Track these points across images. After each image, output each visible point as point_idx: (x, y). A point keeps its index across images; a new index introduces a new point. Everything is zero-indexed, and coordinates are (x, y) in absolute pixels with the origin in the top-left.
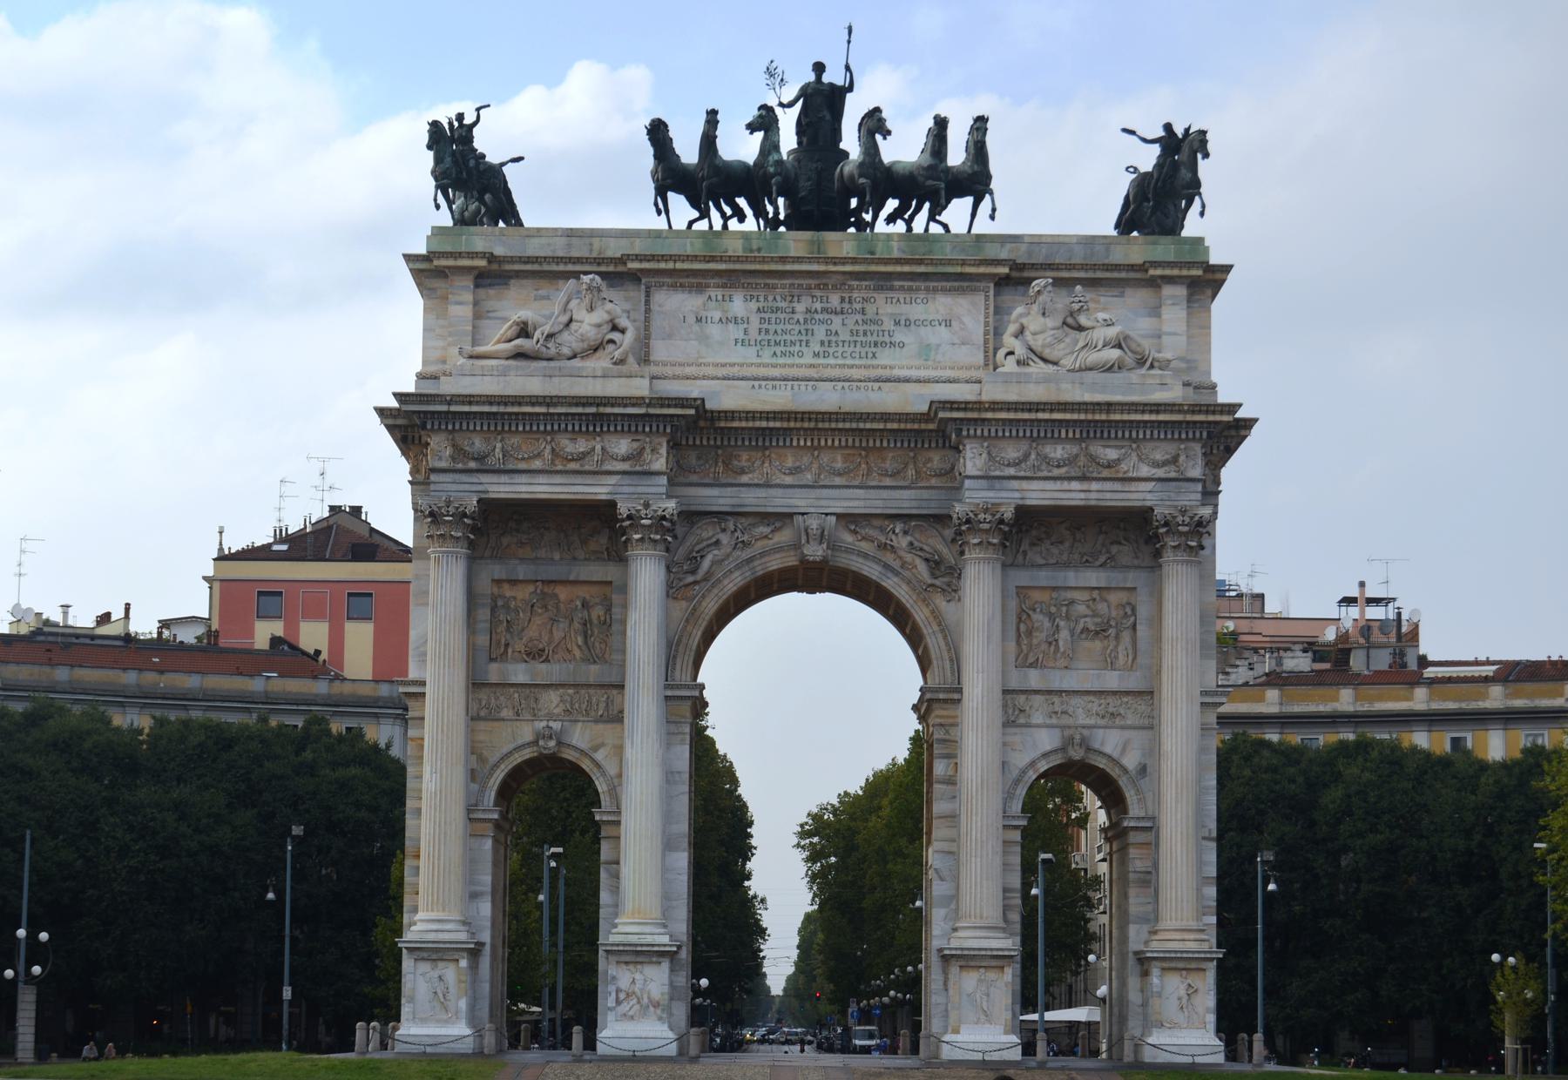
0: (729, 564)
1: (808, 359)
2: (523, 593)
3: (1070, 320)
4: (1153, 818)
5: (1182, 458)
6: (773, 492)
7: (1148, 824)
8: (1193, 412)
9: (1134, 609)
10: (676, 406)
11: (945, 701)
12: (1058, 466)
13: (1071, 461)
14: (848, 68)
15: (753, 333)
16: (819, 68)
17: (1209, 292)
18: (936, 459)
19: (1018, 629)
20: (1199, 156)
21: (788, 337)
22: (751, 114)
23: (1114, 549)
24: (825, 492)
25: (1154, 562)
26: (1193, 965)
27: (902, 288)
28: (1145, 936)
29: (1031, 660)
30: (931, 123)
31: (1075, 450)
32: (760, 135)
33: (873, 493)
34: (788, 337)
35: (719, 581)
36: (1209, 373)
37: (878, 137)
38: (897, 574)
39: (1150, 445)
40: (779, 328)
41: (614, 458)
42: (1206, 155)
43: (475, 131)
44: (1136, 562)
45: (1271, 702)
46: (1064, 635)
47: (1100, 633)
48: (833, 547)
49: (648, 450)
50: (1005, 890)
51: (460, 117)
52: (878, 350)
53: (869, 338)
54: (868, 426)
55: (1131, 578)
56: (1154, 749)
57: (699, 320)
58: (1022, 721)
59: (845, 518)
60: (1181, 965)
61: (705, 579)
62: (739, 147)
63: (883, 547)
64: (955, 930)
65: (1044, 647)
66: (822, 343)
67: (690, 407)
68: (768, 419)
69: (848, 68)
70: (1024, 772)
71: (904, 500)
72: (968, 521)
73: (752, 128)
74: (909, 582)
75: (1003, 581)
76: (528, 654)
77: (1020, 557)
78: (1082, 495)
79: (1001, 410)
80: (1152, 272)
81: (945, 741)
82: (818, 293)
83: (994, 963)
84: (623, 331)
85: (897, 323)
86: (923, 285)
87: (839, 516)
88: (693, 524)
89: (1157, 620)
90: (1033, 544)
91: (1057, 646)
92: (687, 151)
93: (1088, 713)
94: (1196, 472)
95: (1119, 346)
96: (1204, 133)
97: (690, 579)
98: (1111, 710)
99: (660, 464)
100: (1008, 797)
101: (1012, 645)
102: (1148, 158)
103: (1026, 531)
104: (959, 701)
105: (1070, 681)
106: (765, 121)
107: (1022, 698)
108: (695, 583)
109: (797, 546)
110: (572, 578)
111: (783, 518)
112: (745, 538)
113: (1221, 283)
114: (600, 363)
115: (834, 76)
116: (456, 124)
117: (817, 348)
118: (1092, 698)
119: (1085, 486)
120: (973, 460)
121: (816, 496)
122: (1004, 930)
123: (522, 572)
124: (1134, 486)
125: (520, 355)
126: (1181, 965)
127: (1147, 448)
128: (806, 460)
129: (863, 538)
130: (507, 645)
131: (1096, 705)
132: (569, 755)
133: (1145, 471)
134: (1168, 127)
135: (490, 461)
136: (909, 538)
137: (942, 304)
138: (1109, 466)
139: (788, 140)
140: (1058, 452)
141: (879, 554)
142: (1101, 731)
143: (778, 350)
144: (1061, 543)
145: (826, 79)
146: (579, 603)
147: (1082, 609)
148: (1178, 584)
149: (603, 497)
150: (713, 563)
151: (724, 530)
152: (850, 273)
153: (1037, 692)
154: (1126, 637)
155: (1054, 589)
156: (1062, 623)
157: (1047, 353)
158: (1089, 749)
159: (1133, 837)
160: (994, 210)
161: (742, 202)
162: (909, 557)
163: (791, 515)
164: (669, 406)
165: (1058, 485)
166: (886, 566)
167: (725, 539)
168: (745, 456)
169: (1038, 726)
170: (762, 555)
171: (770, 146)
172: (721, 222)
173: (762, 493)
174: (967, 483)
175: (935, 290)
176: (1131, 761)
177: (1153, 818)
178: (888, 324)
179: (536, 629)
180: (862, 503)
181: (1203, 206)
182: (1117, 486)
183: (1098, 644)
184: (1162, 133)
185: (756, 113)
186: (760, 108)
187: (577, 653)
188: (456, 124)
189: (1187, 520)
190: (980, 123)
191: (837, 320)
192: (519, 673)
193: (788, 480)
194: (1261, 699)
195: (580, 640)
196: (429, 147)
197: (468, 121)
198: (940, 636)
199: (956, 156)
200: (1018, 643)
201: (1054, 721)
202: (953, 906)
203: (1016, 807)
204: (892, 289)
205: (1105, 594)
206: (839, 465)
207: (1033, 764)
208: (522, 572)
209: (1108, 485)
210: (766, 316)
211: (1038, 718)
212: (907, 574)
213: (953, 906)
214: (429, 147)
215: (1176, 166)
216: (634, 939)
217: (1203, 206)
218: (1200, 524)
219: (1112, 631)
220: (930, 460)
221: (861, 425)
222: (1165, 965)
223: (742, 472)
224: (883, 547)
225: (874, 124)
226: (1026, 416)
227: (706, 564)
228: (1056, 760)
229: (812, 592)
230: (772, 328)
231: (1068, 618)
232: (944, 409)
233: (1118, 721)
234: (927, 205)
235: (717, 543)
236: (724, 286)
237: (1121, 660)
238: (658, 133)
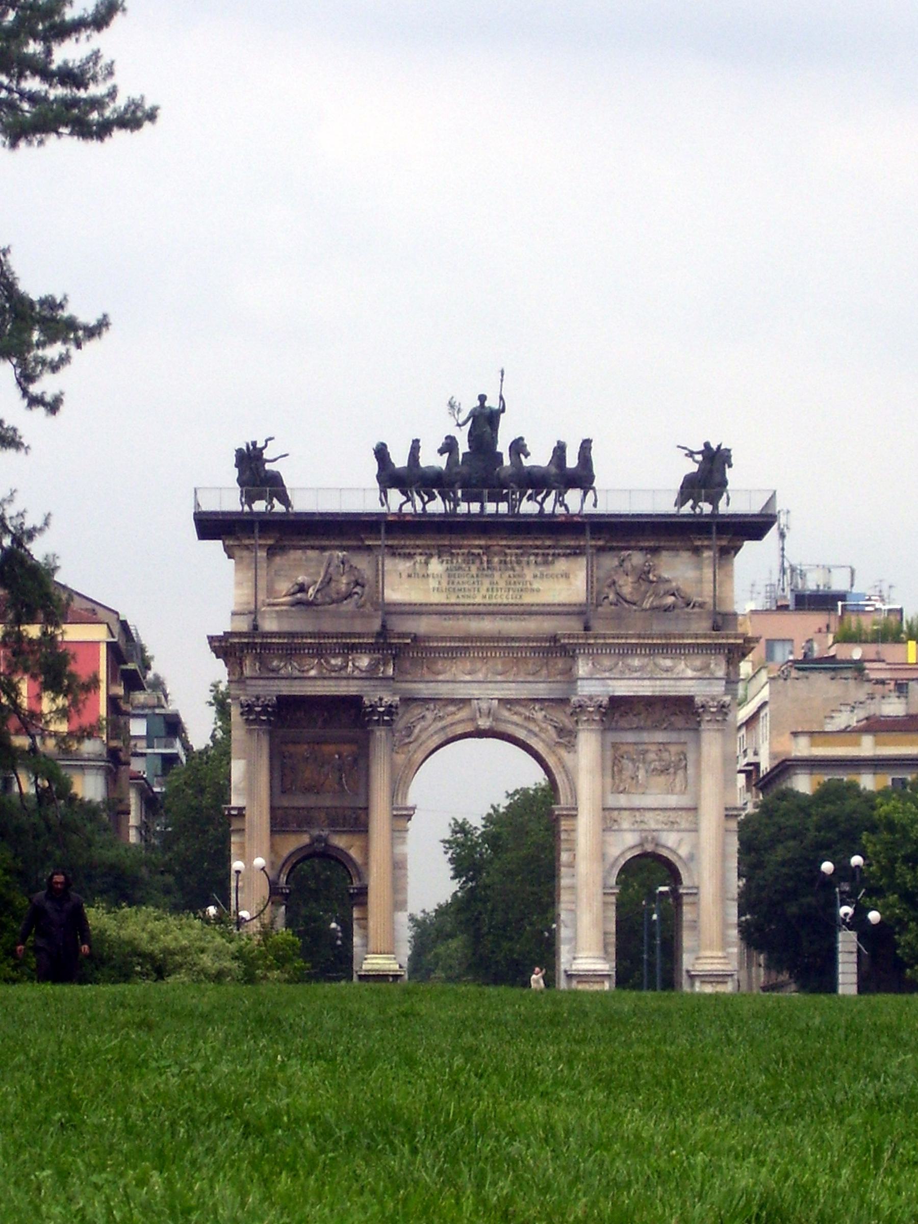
0: (432, 729)
1: (478, 600)
3: (643, 576)
4: (697, 888)
5: (712, 666)
6: (458, 685)
9: (685, 759)
11: (567, 815)
12: (636, 671)
13: (642, 668)
14: (501, 398)
15: (444, 584)
16: (482, 398)
17: (733, 552)
18: (560, 664)
19: (613, 770)
20: (726, 466)
21: (466, 586)
22: (440, 442)
23: (673, 719)
24: (490, 685)
25: (696, 730)
26: (720, 979)
28: (692, 961)
29: (621, 789)
30: (556, 444)
31: (646, 660)
32: (446, 455)
33: (521, 686)
34: (466, 586)
35: (424, 742)
36: (732, 602)
37: (522, 456)
38: (536, 735)
39: (694, 657)
40: (461, 580)
42: (730, 466)
44: (687, 726)
45: (867, 747)
46: (641, 774)
47: (664, 771)
48: (496, 719)
50: (605, 933)
51: (254, 444)
52: (523, 594)
53: (518, 586)
55: (684, 736)
56: (696, 846)
57: (409, 576)
58: (616, 827)
59: (503, 701)
60: (712, 979)
61: (415, 740)
62: (432, 459)
63: (528, 719)
64: (574, 958)
65: (629, 780)
66: (488, 590)
67: (407, 638)
69: (501, 398)
70: (617, 859)
71: (541, 690)
73: (441, 452)
74: (543, 741)
75: (603, 739)
77: (614, 724)
83: (598, 979)
84: (363, 586)
85: (535, 576)
87: (500, 700)
88: (408, 706)
89: (698, 763)
90: (621, 716)
91: (638, 782)
92: (400, 460)
93: (657, 822)
94: (721, 673)
95: (673, 595)
96: (729, 451)
97: (407, 741)
98: (671, 819)
100: (607, 873)
101: (609, 780)
103: (617, 710)
104: (576, 815)
105: (648, 801)
106: (450, 446)
107: (616, 813)
108: (410, 743)
109: (473, 719)
111: (465, 702)
112: (441, 714)
114: (348, 606)
115: (492, 403)
116: (251, 447)
117: (483, 592)
119: (653, 683)
120: (583, 668)
122: (604, 959)
124: (683, 683)
125: (299, 603)
126: (712, 979)
128: (479, 665)
129: (516, 713)
131: (661, 816)
133: (690, 673)
134: (707, 445)
135: (282, 672)
136: (543, 713)
137: (562, 565)
138: (667, 671)
139: (463, 447)
140: (636, 662)
141: (526, 724)
142: (665, 833)
143: (460, 594)
144: (640, 714)
145: (487, 404)
148: (711, 745)
150: (420, 731)
151: (428, 709)
153: (625, 809)
154: (681, 773)
155: (635, 744)
156: (641, 765)
157: (628, 597)
158: (657, 845)
159: (686, 899)
160: (596, 501)
161: (436, 491)
162: (544, 725)
163: (470, 699)
165: (636, 682)
166: (530, 731)
167: (429, 715)
168: (440, 663)
169: (625, 830)
170: (452, 724)
171: (451, 462)
172: (422, 505)
173: (450, 686)
174: (579, 683)
175: (559, 555)
176: (683, 851)
177: (697, 888)
178: (529, 577)
180: (513, 692)
181: (728, 499)
182: (672, 682)
183: (662, 779)
185: (444, 440)
186: (447, 438)
188: (251, 447)
189: (716, 704)
190: (586, 446)
191: (497, 574)
192: (300, 801)
193: (468, 678)
194: (858, 744)
197: (259, 445)
198: (563, 775)
199: (572, 461)
200: (613, 778)
202: (573, 943)
203: (613, 880)
205: (667, 747)
206: (500, 667)
207: (623, 853)
209: (666, 682)
211: (625, 825)
212: (543, 735)
213: (573, 943)
215: (711, 472)
216: (377, 967)
217: (728, 499)
218: (723, 706)
219: (672, 770)
220: (556, 663)
222: (703, 979)
223: (439, 673)
224: (528, 719)
225: (518, 447)
226: (616, 641)
227: (416, 731)
228: (636, 852)
230: (456, 580)
231: (644, 761)
234: (554, 492)
235: (423, 717)
237: (678, 789)
238: (381, 453)
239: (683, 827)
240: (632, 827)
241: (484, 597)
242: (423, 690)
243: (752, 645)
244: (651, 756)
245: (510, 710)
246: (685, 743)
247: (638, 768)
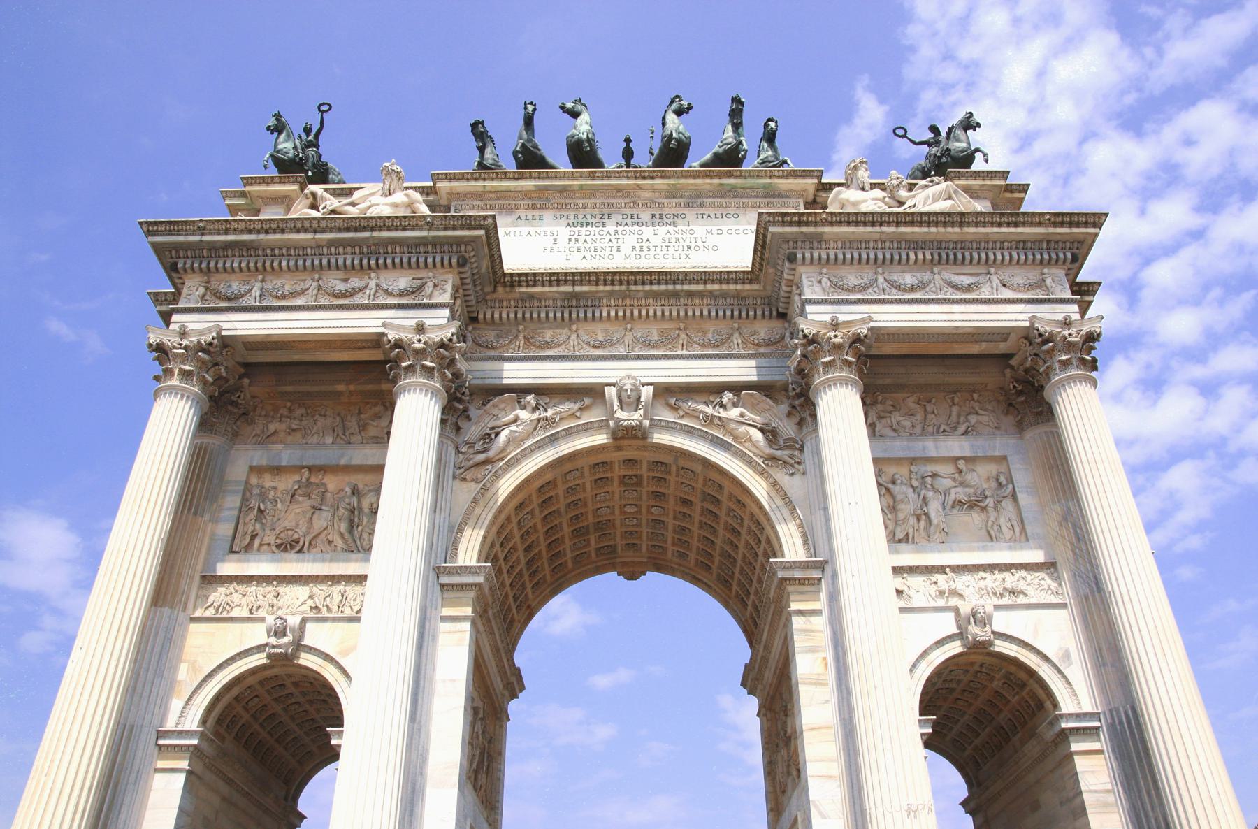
2: (286, 483)
5: (1048, 281)
8: (1055, 224)
10: (462, 227)
11: (802, 581)
23: (973, 419)
27: (712, 206)
29: (900, 535)
40: (588, 238)
41: (387, 293)
46: (934, 508)
47: (974, 504)
54: (686, 287)
55: (1001, 445)
59: (665, 392)
65: (913, 521)
66: (634, 248)
68: (574, 283)
76: (278, 546)
78: (945, 317)
79: (840, 223)
81: (806, 631)
82: (629, 212)
86: (733, 201)
90: (880, 418)
91: (930, 522)
95: (950, 198)
97: (482, 457)
98: (1009, 585)
99: (446, 298)
110: (343, 462)
111: (592, 393)
118: (982, 574)
123: (286, 456)
127: (1006, 274)
129: (686, 415)
130: (253, 537)
143: (588, 254)
146: (348, 490)
147: (946, 483)
150: (508, 443)
151: (523, 408)
152: (660, 191)
155: (913, 461)
156: (930, 494)
164: (454, 228)
167: (524, 415)
179: (292, 518)
183: (976, 517)
184: (929, 135)
187: (339, 542)
195: (343, 527)
201: (941, 602)
204: (701, 206)
207: (924, 654)
208: (286, 456)
210: (576, 230)
217: (985, 155)
219: (990, 502)
220: (755, 333)
221: (678, 287)
223: (547, 346)
224: (709, 420)
228: (956, 648)
229: (632, 574)
232: (774, 223)
233: (1021, 600)
236: (534, 207)
239: (1033, 601)
240: (933, 604)
241: (627, 257)
242: (515, 373)
244: (946, 483)
245: (675, 408)
246: (1004, 458)
247: (924, 499)
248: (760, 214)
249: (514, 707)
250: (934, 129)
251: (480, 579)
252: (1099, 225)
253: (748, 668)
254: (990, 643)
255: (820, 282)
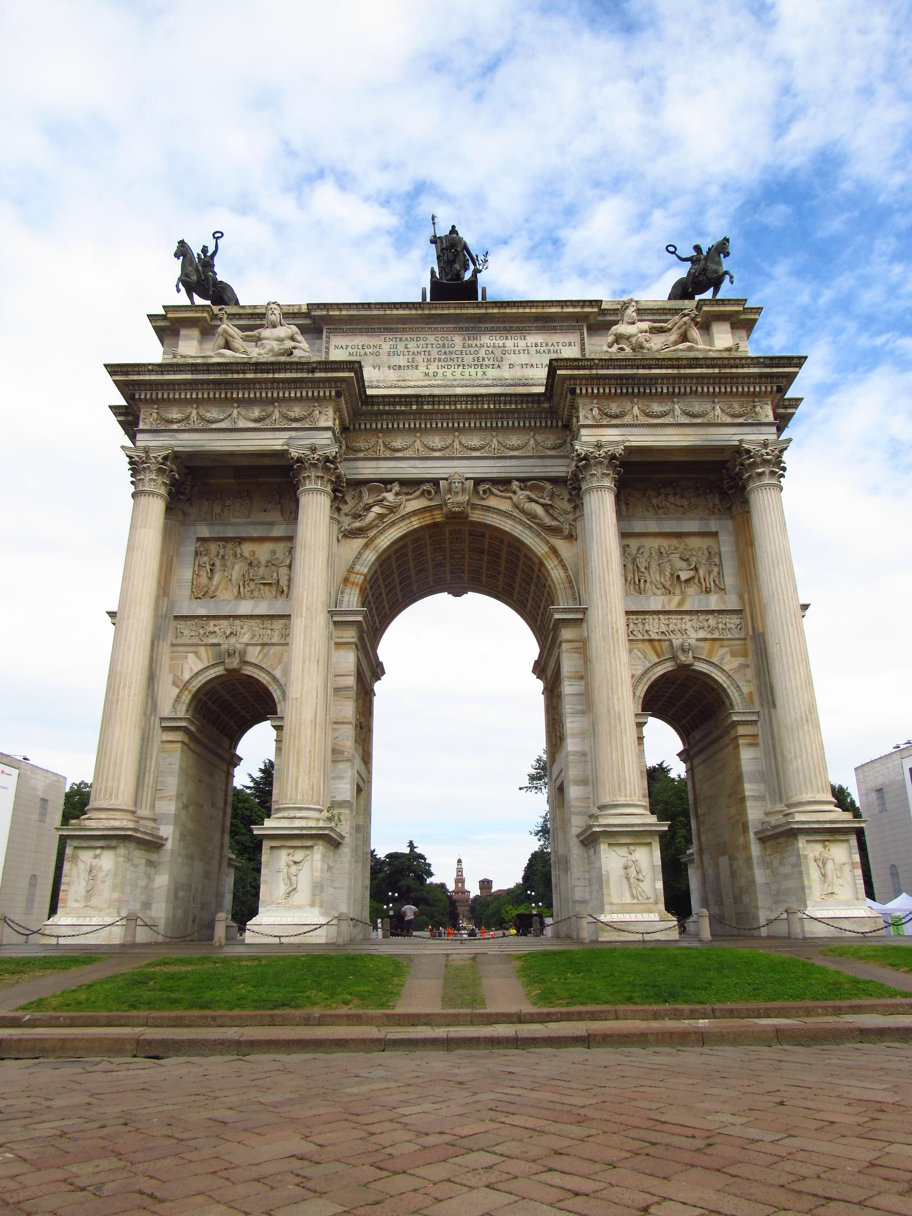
7: (754, 718)
20: (722, 255)
43: (216, 258)
49: (317, 412)
67: (350, 371)
72: (586, 458)
80: (705, 308)
87: (478, 482)
102: (681, 272)
104: (581, 620)
113: (755, 321)
121: (456, 463)
132: (248, 671)
149: (279, 448)
196: (177, 255)
214: (177, 255)
217: (731, 277)
229: (457, 592)
243: (790, 411)
248: (551, 361)
249: (378, 686)
250: (697, 248)
251: (360, 618)
252: (800, 366)
253: (537, 663)
254: (692, 665)
255: (591, 410)
